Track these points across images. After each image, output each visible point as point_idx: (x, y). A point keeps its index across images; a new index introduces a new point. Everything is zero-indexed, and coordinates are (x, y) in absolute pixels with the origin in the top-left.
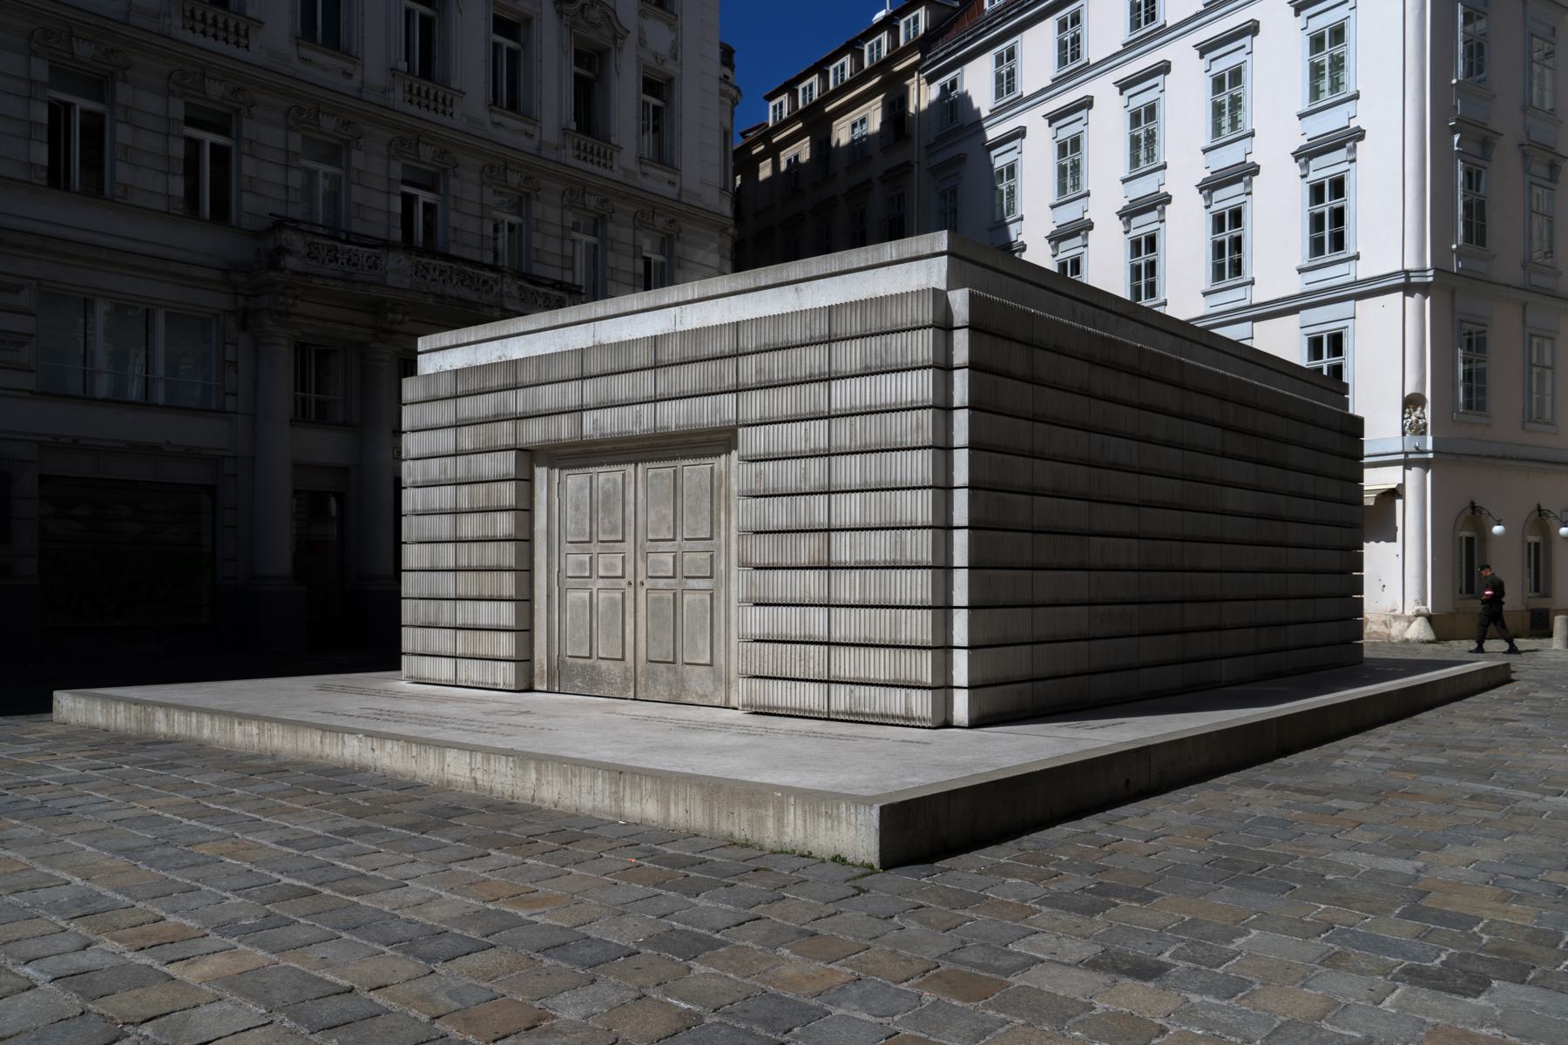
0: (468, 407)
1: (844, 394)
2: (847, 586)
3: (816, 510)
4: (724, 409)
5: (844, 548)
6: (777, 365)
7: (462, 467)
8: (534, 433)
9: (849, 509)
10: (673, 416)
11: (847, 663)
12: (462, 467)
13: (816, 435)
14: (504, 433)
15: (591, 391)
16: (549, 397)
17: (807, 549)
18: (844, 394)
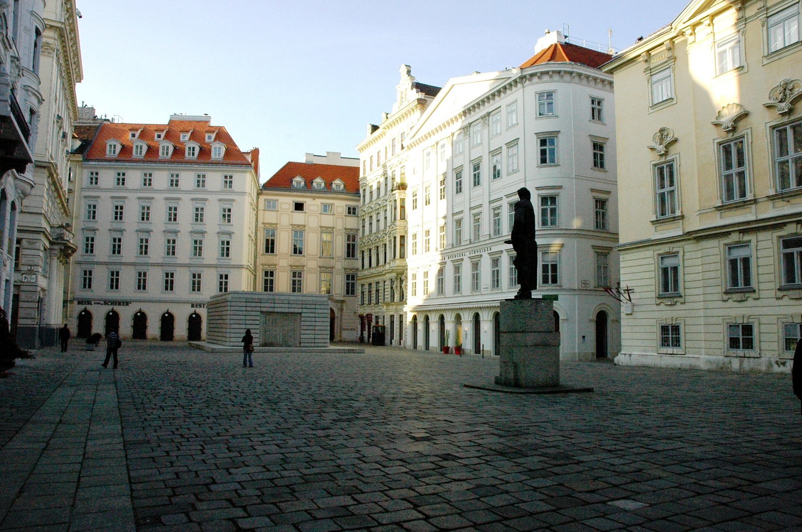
0: (248, 304)
1: (317, 311)
2: (317, 332)
3: (313, 324)
4: (300, 311)
5: (317, 328)
6: (308, 306)
7: (248, 313)
8: (264, 310)
9: (317, 324)
10: (291, 310)
11: (317, 341)
12: (248, 313)
13: (313, 315)
14: (258, 309)
15: (276, 305)
16: (267, 305)
17: (312, 328)
18: (317, 311)
